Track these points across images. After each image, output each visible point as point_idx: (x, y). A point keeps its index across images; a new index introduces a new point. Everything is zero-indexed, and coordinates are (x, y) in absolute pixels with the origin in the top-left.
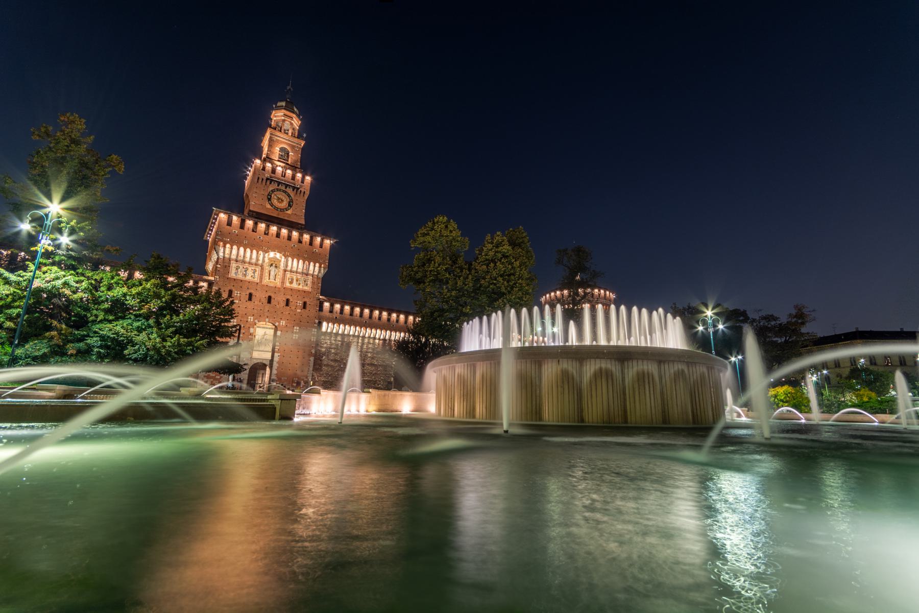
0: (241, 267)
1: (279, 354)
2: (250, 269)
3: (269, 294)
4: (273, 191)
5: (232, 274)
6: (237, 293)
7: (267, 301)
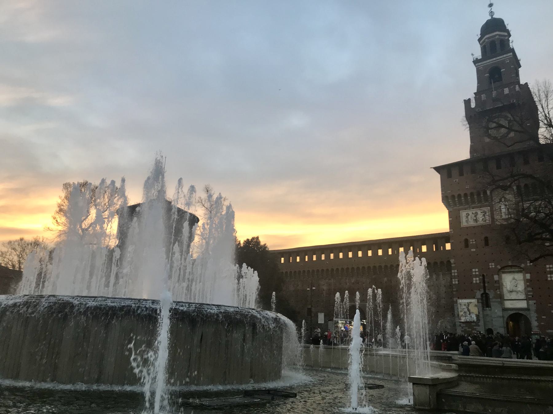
0: (470, 213)
1: (535, 302)
2: (479, 212)
5: (464, 224)
6: (473, 242)
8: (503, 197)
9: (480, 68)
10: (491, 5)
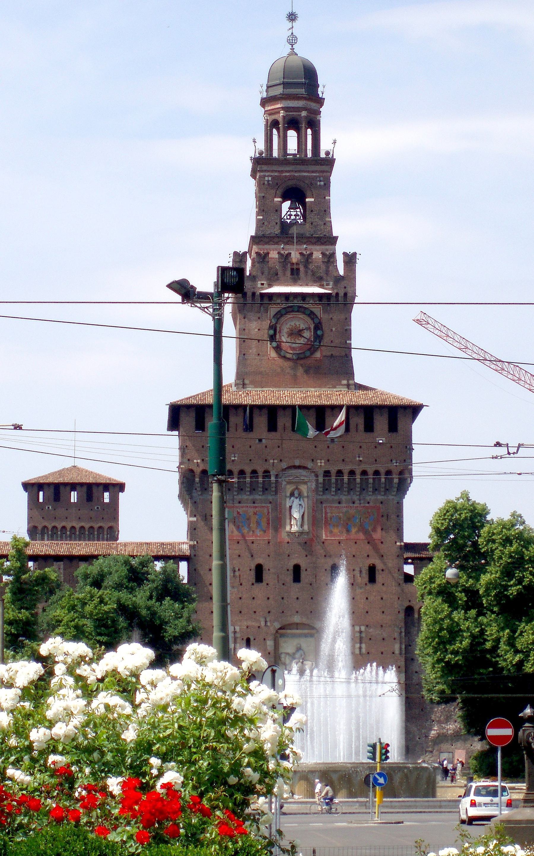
3: (295, 562)
4: (279, 315)
7: (292, 577)
8: (297, 488)
9: (266, 179)
10: (292, 17)
